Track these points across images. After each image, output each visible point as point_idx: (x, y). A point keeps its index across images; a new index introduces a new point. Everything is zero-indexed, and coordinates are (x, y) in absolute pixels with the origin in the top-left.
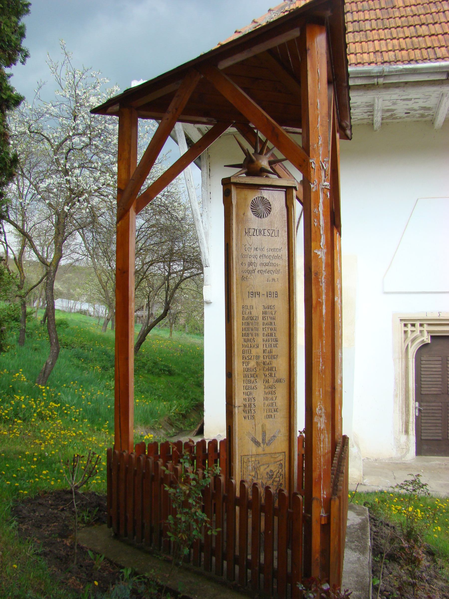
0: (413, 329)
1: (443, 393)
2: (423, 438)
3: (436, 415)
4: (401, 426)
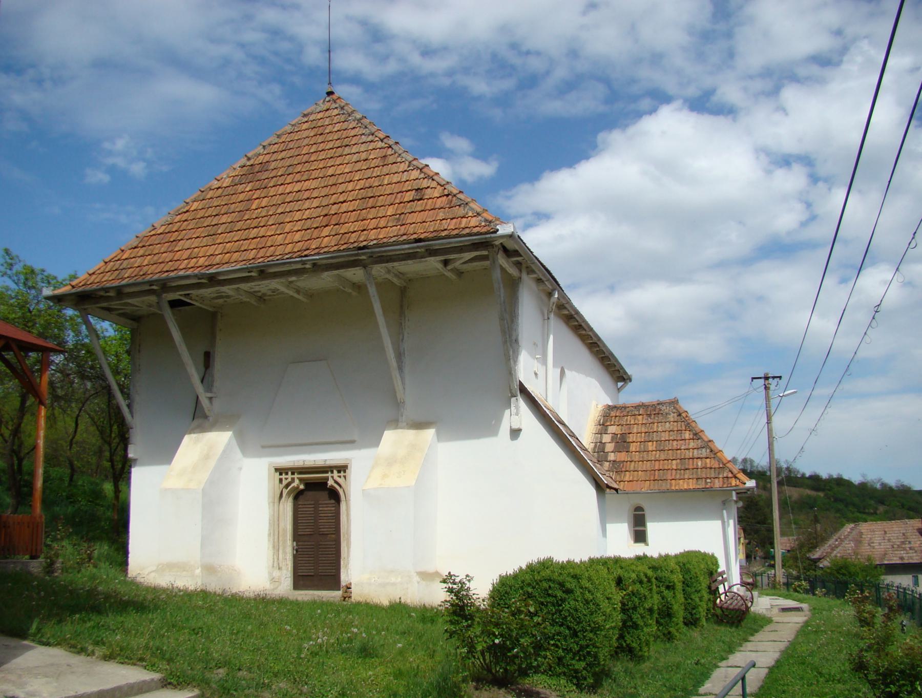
0: (287, 476)
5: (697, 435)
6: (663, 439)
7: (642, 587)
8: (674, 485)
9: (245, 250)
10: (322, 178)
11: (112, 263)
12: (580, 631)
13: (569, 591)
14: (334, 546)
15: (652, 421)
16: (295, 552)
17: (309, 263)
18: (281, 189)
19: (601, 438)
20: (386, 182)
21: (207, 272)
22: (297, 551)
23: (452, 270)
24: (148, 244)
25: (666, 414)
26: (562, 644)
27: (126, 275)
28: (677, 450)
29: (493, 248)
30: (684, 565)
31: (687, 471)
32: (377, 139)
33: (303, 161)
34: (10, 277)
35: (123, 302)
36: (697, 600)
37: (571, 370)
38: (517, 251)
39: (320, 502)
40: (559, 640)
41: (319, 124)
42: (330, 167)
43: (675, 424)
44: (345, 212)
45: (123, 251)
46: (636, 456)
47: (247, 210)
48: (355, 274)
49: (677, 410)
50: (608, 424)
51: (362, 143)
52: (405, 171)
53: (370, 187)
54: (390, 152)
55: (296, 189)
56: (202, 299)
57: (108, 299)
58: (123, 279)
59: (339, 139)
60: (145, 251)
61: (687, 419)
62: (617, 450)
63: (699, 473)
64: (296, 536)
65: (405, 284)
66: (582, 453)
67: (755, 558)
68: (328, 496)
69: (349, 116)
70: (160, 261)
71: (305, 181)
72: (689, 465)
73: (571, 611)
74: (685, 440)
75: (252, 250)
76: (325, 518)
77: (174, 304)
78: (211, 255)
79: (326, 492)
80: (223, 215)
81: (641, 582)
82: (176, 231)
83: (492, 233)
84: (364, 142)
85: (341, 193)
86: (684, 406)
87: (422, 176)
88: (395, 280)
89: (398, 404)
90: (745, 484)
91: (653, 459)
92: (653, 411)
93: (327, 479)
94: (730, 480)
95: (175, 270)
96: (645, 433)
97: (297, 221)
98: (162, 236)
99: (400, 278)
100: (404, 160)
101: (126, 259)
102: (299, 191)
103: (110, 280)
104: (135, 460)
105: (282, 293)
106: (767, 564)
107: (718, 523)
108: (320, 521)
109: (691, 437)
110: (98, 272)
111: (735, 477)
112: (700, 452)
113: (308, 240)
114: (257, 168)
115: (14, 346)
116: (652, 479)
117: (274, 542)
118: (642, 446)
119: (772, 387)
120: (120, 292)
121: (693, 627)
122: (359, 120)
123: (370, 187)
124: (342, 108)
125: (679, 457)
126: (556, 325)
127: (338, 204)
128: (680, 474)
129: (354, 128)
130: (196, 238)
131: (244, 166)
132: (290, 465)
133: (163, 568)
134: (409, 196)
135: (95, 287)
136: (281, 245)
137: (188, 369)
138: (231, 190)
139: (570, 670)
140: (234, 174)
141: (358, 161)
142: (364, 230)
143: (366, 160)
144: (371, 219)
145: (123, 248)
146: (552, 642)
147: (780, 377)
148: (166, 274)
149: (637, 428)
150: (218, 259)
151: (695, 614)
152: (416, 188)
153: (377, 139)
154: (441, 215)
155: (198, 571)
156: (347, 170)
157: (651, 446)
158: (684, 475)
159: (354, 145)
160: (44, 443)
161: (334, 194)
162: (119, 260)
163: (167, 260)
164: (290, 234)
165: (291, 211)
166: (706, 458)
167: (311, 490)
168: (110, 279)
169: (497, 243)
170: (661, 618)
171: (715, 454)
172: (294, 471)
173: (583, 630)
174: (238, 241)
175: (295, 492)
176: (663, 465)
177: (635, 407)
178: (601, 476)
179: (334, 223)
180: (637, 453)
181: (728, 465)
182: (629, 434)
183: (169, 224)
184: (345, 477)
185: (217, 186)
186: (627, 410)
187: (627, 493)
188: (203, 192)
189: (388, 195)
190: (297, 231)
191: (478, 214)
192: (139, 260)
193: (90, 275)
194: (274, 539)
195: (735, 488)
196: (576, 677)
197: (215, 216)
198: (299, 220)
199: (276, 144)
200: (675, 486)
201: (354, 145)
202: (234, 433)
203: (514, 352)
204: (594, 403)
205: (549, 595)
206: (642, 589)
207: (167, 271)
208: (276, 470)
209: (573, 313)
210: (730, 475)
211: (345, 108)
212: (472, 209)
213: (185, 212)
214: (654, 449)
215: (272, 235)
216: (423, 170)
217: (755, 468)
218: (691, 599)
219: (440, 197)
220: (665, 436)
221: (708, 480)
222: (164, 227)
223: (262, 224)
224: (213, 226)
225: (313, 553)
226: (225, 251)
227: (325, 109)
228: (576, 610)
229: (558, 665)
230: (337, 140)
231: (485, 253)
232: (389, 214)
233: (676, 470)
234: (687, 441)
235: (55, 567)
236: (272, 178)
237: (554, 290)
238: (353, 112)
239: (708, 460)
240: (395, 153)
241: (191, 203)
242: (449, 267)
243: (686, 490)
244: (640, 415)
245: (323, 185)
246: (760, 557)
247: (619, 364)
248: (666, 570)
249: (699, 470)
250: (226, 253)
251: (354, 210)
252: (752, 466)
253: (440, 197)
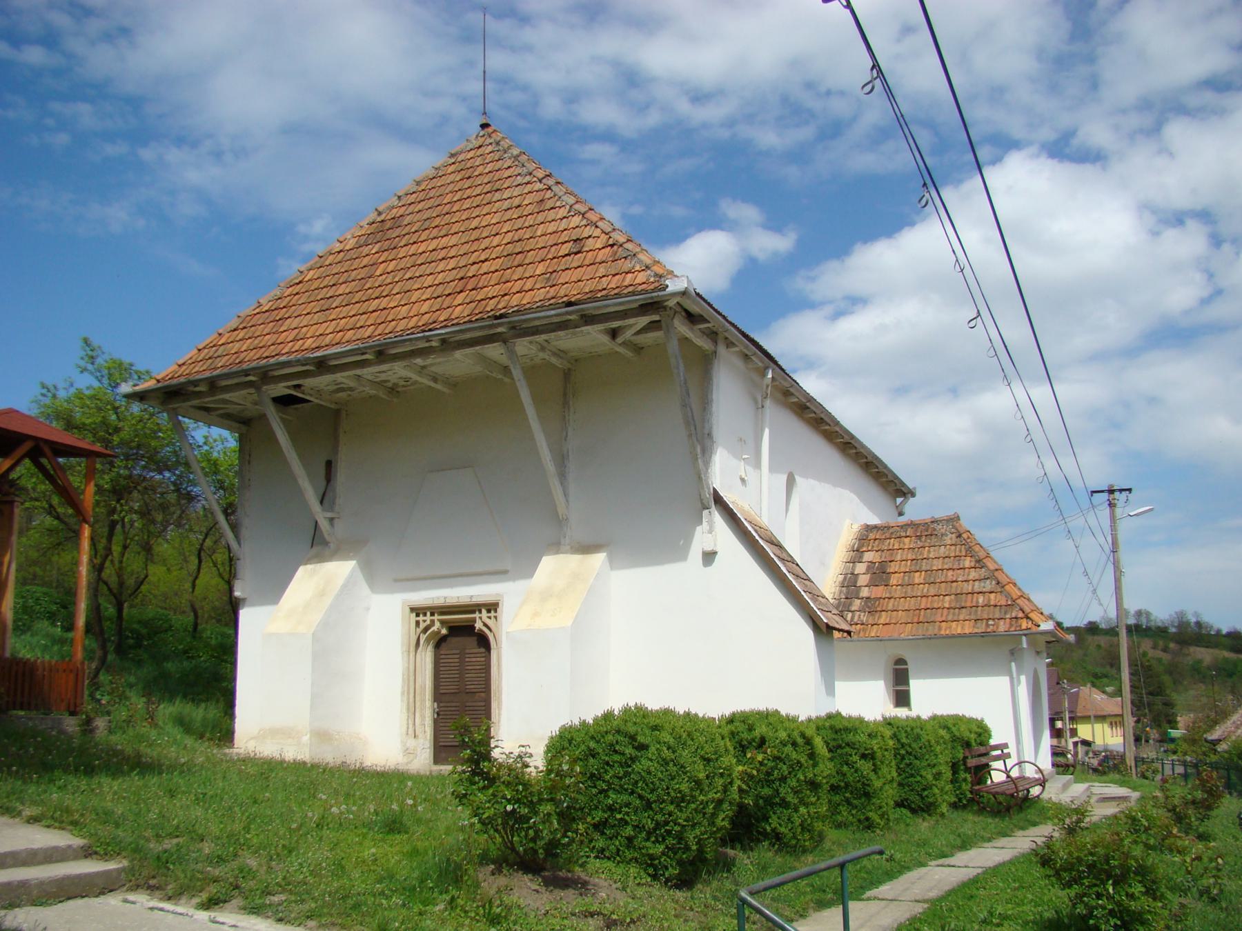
0: (425, 618)
5: (979, 564)
6: (935, 568)
7: (796, 751)
8: (944, 628)
9: (361, 327)
10: (463, 232)
11: (206, 351)
12: (655, 801)
13: (643, 747)
14: (483, 708)
15: (921, 544)
16: (436, 716)
17: (433, 339)
18: (413, 249)
19: (853, 568)
20: (539, 233)
21: (312, 356)
22: (438, 714)
23: (624, 344)
24: (250, 325)
25: (942, 535)
26: (631, 819)
27: (219, 365)
28: (952, 582)
29: (666, 310)
30: (912, 729)
31: (964, 610)
32: (535, 179)
33: (444, 212)
34: (92, 373)
35: (217, 398)
36: (930, 777)
37: (805, 476)
38: (702, 316)
39: (467, 651)
40: (627, 814)
41: (468, 166)
42: (474, 218)
43: (953, 547)
44: (485, 273)
45: (220, 334)
46: (898, 592)
47: (369, 277)
48: (495, 351)
49: (957, 529)
50: (864, 549)
51: (516, 186)
52: (564, 218)
53: (520, 240)
54: (549, 194)
55: (430, 248)
56: (319, 392)
57: (199, 395)
58: (215, 369)
59: (489, 182)
60: (246, 334)
61: (969, 540)
62: (872, 584)
63: (979, 613)
64: (438, 696)
65: (570, 366)
66: (794, 583)
67: (1147, 741)
68: (476, 642)
69: (505, 152)
70: (261, 345)
71: (442, 237)
72: (966, 601)
73: (643, 774)
74: (964, 569)
75: (369, 326)
77: (284, 402)
78: (321, 335)
79: (475, 638)
80: (341, 284)
81: (794, 744)
82: (284, 307)
83: (660, 290)
84: (519, 185)
85: (484, 250)
86: (965, 523)
87: (584, 222)
88: (554, 360)
89: (560, 522)
90: (1039, 626)
91: (919, 594)
92: (925, 531)
93: (474, 620)
94: (1020, 621)
95: (276, 355)
96: (912, 560)
97: (427, 288)
98: (267, 313)
99: (561, 357)
100: (564, 203)
101: (223, 344)
102: (434, 250)
103: (201, 371)
104: (244, 600)
105: (416, 382)
106: (1162, 749)
107: (1006, 679)
108: (467, 675)
109: (973, 564)
110: (190, 362)
111: (1027, 618)
112: (982, 584)
113: (437, 310)
114: (388, 225)
115: (47, 450)
116: (916, 620)
117: (408, 703)
118: (906, 578)
119: (1120, 504)
120: (213, 384)
121: (926, 815)
122: (516, 157)
123: (520, 240)
124: (498, 143)
125: (953, 591)
126: (777, 417)
127: (478, 263)
128: (954, 614)
129: (509, 167)
130: (306, 315)
131: (373, 223)
132: (429, 603)
133: (275, 732)
134: (565, 249)
135: (182, 380)
136: (404, 318)
137: (300, 481)
138: (353, 254)
139: (643, 855)
140: (360, 234)
141: (508, 209)
142: (506, 295)
143: (519, 206)
144: (516, 281)
145: (221, 331)
146: (619, 816)
147: (1130, 490)
148: (265, 361)
149: (902, 555)
150: (328, 339)
151: (927, 796)
152: (575, 238)
153: (535, 179)
154: (602, 270)
155: (306, 739)
156: (494, 221)
157: (918, 578)
158: (959, 615)
159: (506, 189)
160: (88, 570)
161: (475, 251)
162: (214, 346)
163: (269, 343)
164: (416, 304)
165: (421, 276)
166: (991, 593)
167: (457, 636)
168: (201, 369)
169: (672, 303)
170: (855, 799)
171: (1003, 587)
172: (434, 610)
173: (658, 800)
174: (354, 315)
175: (437, 638)
176: (932, 602)
177: (902, 527)
178: (819, 613)
179: (470, 288)
180: (899, 587)
181: (1019, 601)
182: (890, 562)
183: (277, 300)
184: (496, 617)
185: (338, 250)
186: (891, 530)
187: (881, 640)
188: (321, 257)
189: (540, 249)
190: (425, 301)
191: (648, 267)
192: (237, 345)
193: (180, 366)
194: (408, 699)
195: (1025, 632)
196: (652, 865)
197: (331, 286)
198: (430, 286)
199: (414, 193)
200: (946, 630)
201: (506, 189)
202: (359, 563)
203: (704, 451)
204: (848, 522)
205: (616, 752)
206: (794, 752)
207: (267, 357)
208: (412, 610)
209: (804, 400)
210: (1021, 615)
211: (502, 143)
212: (640, 262)
213: (298, 284)
214: (922, 581)
215: (395, 307)
216: (585, 216)
217: (1153, 624)
218: (921, 776)
219: (603, 248)
220: (937, 564)
221: (991, 622)
222: (271, 303)
223: (384, 294)
224: (328, 298)
226: (338, 329)
227: (477, 146)
228: (649, 773)
229: (628, 847)
230: (486, 184)
231: (656, 318)
232: (538, 272)
233: (948, 609)
234: (967, 570)
235: (94, 725)
236: (404, 235)
237: (767, 368)
238: (509, 148)
239: (992, 596)
240: (555, 195)
241: (306, 272)
242: (620, 340)
243: (960, 636)
244: (906, 537)
245: (463, 241)
246: (1154, 739)
247: (891, 471)
248: (863, 733)
249: (980, 608)
250: (338, 332)
251: (496, 271)
252: (1148, 620)
253: (603, 248)
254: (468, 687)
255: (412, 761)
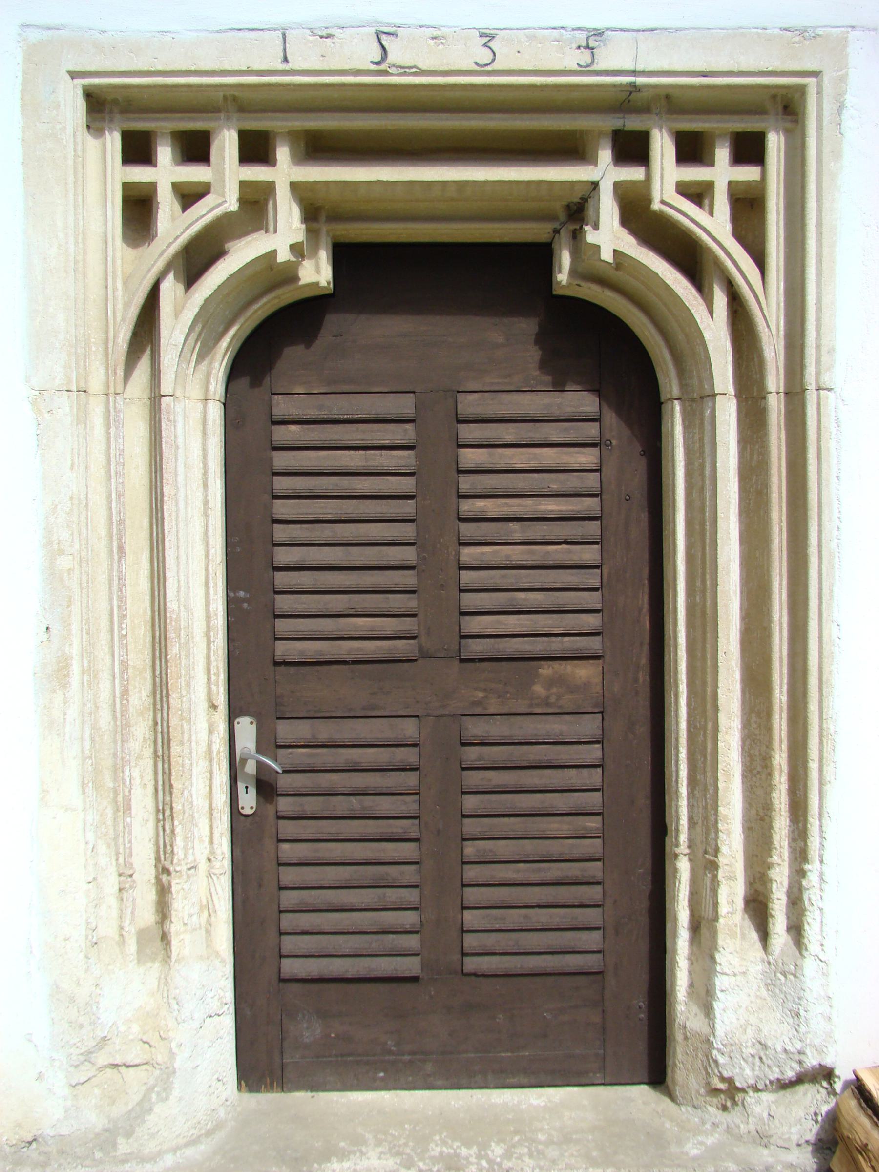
0: (195, 173)
1: (425, 654)
2: (290, 967)
3: (385, 805)
4: (113, 901)
16: (248, 801)
39: (469, 405)
68: (533, 354)
76: (516, 531)
225: (409, 805)
254: (475, 625)
255: (143, 1108)
